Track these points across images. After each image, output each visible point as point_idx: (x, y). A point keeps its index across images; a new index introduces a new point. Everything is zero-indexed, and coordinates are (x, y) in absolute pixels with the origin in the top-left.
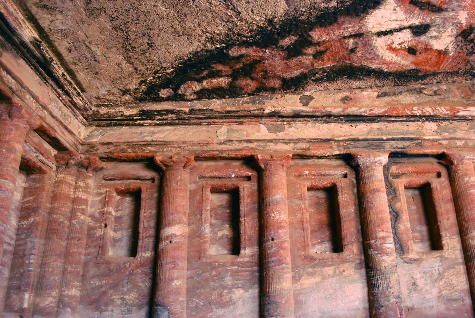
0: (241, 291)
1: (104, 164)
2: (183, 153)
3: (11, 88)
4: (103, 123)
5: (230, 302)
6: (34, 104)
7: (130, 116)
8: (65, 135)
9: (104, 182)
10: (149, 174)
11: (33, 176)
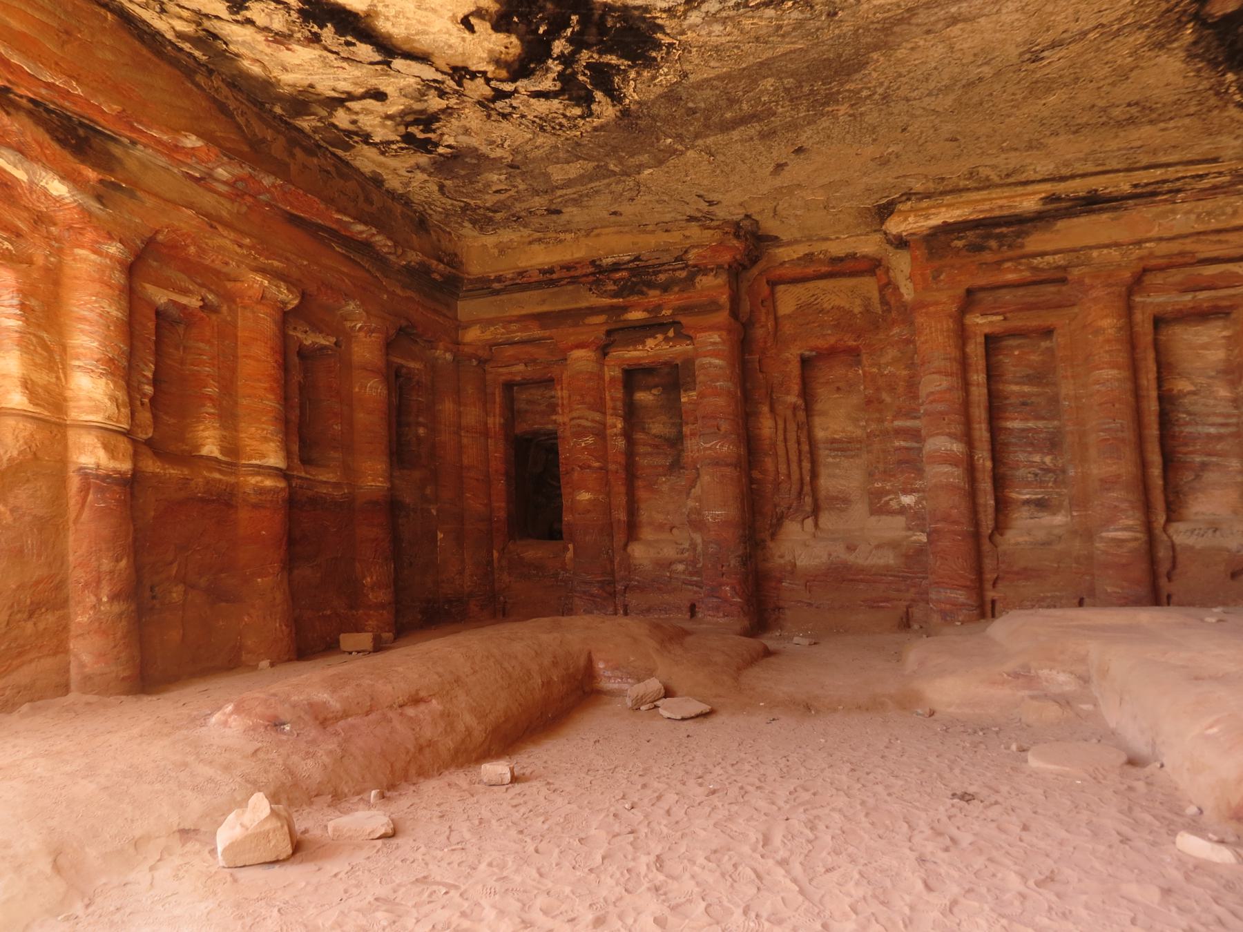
3: (1058, 268)
6: (1115, 253)
8: (1227, 242)
11: (1233, 316)
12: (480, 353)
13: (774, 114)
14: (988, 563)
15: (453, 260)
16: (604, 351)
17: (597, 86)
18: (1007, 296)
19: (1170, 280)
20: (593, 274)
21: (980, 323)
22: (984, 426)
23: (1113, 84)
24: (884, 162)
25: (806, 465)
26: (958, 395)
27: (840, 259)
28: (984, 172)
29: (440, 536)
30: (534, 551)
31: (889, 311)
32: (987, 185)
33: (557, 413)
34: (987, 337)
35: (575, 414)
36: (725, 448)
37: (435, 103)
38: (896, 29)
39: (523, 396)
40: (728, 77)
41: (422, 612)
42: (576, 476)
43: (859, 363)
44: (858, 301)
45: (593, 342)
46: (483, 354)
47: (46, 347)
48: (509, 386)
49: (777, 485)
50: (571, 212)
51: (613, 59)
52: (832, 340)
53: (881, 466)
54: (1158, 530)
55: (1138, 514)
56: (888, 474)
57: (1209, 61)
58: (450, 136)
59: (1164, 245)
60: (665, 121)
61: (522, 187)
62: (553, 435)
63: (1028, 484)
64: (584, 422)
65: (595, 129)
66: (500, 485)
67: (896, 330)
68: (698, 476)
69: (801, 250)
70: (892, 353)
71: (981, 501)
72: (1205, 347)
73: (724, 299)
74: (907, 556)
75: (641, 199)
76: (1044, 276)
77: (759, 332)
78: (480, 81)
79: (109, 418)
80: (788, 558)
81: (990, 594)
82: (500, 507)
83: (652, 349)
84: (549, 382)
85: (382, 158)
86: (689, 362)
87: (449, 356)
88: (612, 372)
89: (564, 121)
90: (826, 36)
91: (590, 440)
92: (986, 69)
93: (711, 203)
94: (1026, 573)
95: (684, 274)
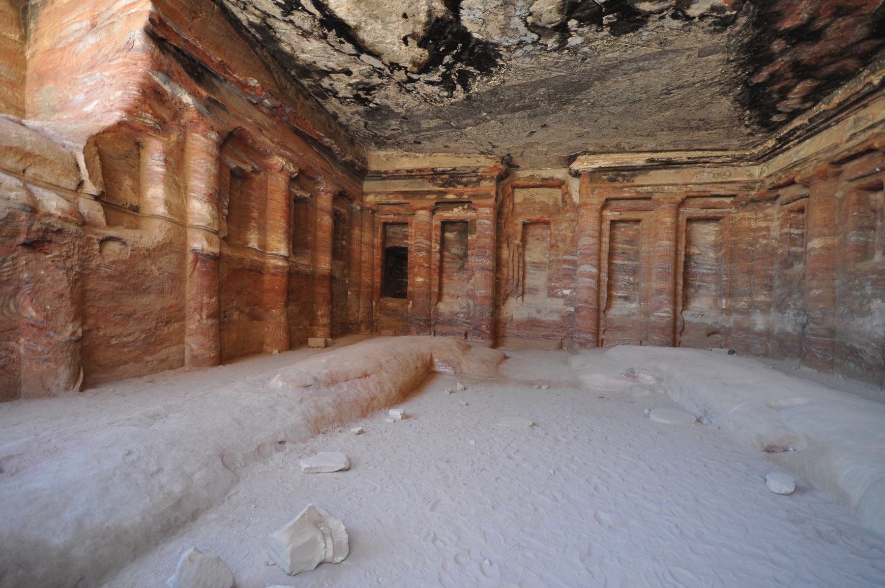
0: (879, 301)
1: (780, 192)
2: (819, 164)
4: (765, 159)
5: (870, 312)
6: (675, 188)
7: (774, 146)
9: (785, 206)
10: (805, 191)
12: (373, 208)
13: (539, 107)
14: (602, 323)
15: (364, 161)
16: (433, 211)
17: (459, 82)
18: (623, 203)
19: (697, 203)
21: (609, 215)
22: (606, 262)
23: (697, 110)
24: (580, 136)
25: (521, 273)
26: (596, 247)
27: (547, 179)
28: (623, 145)
29: (349, 293)
30: (392, 303)
31: (566, 205)
32: (622, 151)
33: (407, 239)
34: (611, 221)
35: (418, 241)
36: (488, 263)
37: (376, 80)
38: (611, 71)
39: (391, 230)
40: (524, 86)
41: (342, 330)
42: (416, 269)
43: (549, 228)
44: (552, 200)
46: (375, 208)
47: (176, 184)
48: (385, 224)
49: (507, 280)
50: (426, 144)
51: (471, 69)
52: (538, 217)
53: (555, 276)
54: (678, 314)
55: (672, 306)
56: (559, 280)
57: (742, 104)
58: (378, 98)
59: (697, 186)
60: (486, 104)
61: (405, 129)
62: (406, 249)
63: (622, 289)
64: (422, 245)
65: (452, 104)
66: (378, 271)
67: (568, 215)
68: (473, 274)
70: (565, 225)
71: (601, 295)
72: (706, 234)
73: (493, 193)
74: (563, 317)
75: (461, 141)
76: (641, 196)
77: (506, 210)
78: (403, 72)
79: (209, 224)
80: (510, 314)
81: (602, 337)
82: (378, 281)
84: (405, 224)
85: (340, 106)
86: (474, 221)
87: (359, 208)
88: (436, 222)
89: (437, 98)
90: (577, 70)
91: (424, 253)
92: (644, 96)
93: (494, 147)
94: (618, 328)
95: (475, 179)
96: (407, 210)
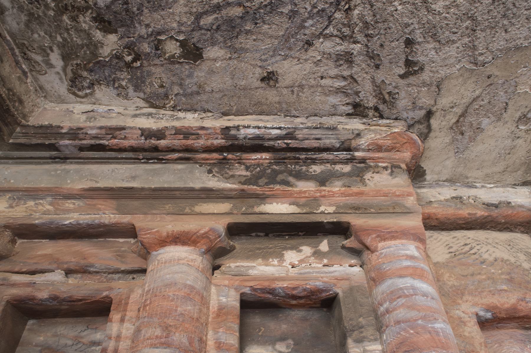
16: (217, 255)
20: (219, 149)
45: (205, 236)
69: (447, 193)
83: (293, 266)
88: (225, 296)
95: (347, 168)
96: (121, 256)
